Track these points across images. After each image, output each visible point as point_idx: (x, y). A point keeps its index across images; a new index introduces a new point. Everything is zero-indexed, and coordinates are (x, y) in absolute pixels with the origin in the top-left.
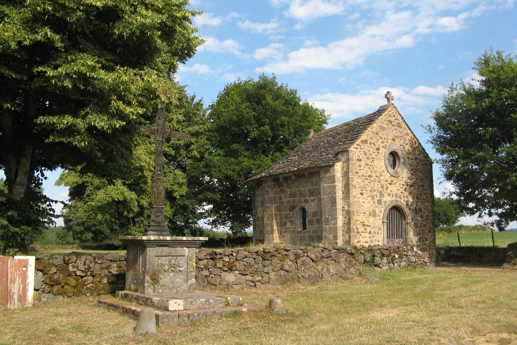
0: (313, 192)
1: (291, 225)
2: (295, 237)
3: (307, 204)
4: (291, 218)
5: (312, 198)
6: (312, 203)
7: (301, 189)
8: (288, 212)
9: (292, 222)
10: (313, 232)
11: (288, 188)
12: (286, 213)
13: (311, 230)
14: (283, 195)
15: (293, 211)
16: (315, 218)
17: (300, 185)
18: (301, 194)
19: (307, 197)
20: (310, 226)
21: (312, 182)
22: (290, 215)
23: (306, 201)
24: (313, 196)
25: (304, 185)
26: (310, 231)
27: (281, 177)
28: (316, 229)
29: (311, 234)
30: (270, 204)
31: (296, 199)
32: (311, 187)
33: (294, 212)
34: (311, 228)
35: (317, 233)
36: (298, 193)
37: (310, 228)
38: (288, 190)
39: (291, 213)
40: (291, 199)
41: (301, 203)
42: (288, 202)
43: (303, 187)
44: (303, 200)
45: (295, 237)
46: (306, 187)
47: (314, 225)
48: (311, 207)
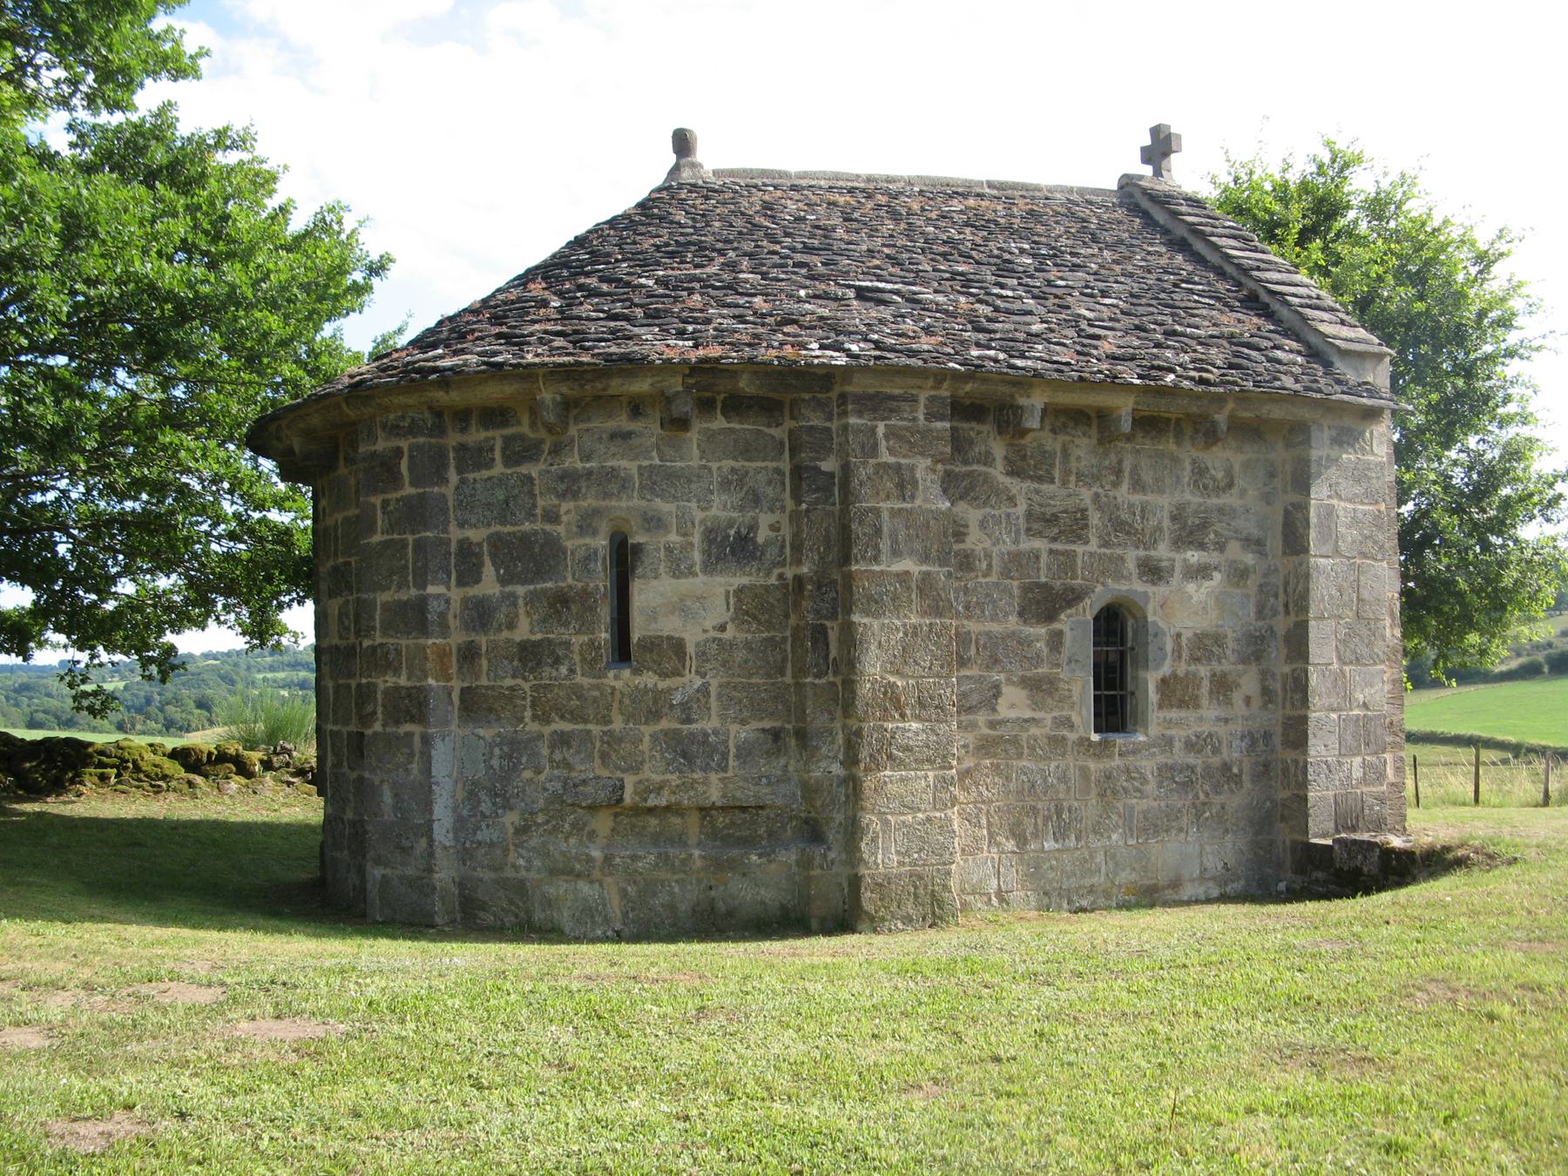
0: (1204, 526)
1: (1036, 705)
2: (1063, 779)
3: (1162, 590)
4: (1037, 660)
5: (1194, 556)
6: (1191, 587)
7: (1124, 493)
8: (1013, 622)
9: (1041, 688)
10: (1190, 746)
11: (1014, 472)
12: (995, 627)
13: (1179, 734)
14: (972, 515)
15: (1051, 617)
16: (1203, 671)
17: (1118, 472)
18: (1120, 526)
19: (1163, 551)
20: (1174, 714)
21: (1200, 471)
22: (1026, 642)
23: (1153, 572)
24: (1202, 546)
25: (1147, 477)
26: (1168, 742)
27: (1036, 401)
28: (1205, 728)
29: (1179, 756)
30: (925, 558)
31: (1080, 549)
32: (1193, 499)
33: (1064, 622)
34: (1178, 724)
35: (1216, 751)
36: (1095, 518)
37: (1169, 723)
38: (1017, 487)
39: (1042, 630)
40: (1040, 544)
41: (1119, 576)
42: (1018, 562)
43: (1138, 485)
44: (1131, 565)
45: (1063, 779)
46: (1160, 491)
47: (1197, 706)
48: (1189, 607)
